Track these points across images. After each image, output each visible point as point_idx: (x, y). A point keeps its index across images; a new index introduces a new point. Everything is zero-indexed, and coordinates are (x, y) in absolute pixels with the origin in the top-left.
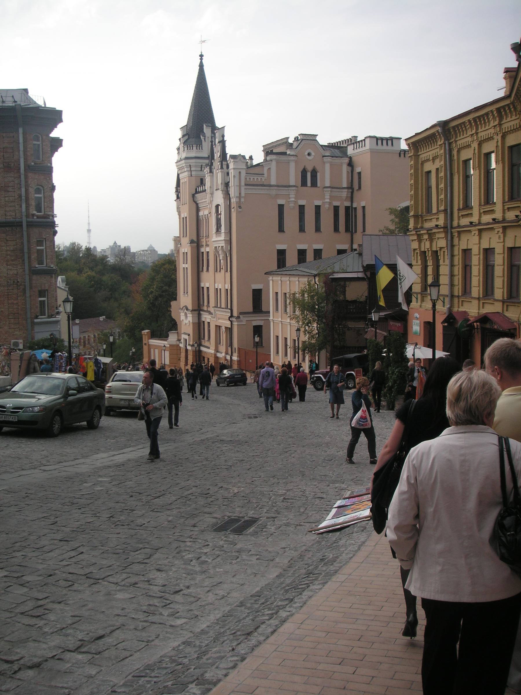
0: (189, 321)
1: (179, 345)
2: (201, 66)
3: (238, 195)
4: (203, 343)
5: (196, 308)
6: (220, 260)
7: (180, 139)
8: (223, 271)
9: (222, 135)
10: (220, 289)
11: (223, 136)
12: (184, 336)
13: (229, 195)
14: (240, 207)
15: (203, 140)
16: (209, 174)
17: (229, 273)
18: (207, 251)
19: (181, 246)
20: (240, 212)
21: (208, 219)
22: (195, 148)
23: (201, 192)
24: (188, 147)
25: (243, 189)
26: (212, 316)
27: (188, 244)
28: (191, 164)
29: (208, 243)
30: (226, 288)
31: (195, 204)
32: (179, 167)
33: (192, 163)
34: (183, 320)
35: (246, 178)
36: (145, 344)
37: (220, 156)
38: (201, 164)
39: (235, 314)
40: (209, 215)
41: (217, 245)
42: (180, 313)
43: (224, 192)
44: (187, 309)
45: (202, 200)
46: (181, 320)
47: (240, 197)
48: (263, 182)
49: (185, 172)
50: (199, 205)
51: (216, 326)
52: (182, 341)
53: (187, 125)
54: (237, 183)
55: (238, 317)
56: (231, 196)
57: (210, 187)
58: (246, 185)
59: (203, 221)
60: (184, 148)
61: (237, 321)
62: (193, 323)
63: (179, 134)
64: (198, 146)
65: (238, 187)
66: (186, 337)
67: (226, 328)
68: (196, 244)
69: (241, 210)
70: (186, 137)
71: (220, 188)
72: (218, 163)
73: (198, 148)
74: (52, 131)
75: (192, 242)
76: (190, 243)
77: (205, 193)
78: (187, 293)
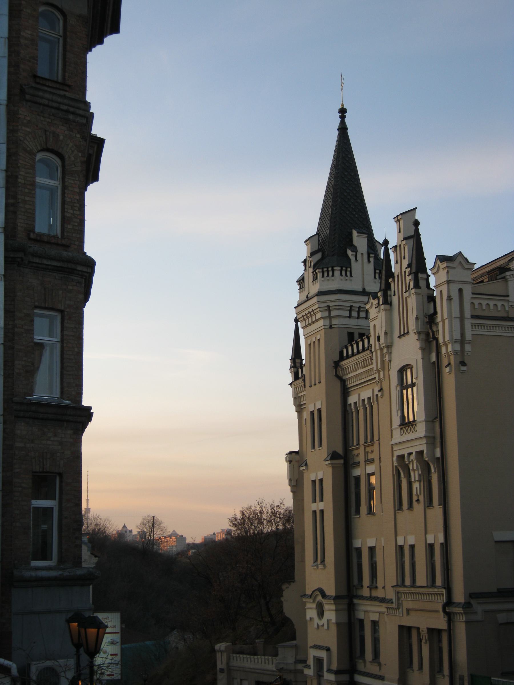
0: (328, 621)
1: (302, 672)
2: (343, 129)
3: (459, 337)
4: (361, 667)
5: (344, 592)
6: (410, 485)
7: (305, 262)
8: (419, 508)
9: (413, 220)
10: (412, 547)
11: (417, 223)
12: (313, 653)
13: (437, 340)
14: (463, 363)
15: (353, 259)
16: (382, 307)
17: (437, 511)
18: (367, 472)
19: (307, 469)
20: (463, 372)
21: (371, 407)
22: (337, 273)
23: (353, 355)
24: (323, 272)
25: (468, 323)
26: (390, 605)
27: (325, 461)
28: (331, 304)
29: (370, 456)
30: (430, 540)
31: (338, 383)
32: (304, 314)
33: (331, 301)
34: (311, 619)
35: (473, 303)
36: (222, 671)
37: (409, 266)
38: (349, 304)
39: (459, 596)
40: (380, 394)
41: (405, 452)
42: (304, 604)
43: (423, 336)
44: (324, 595)
45: (356, 371)
46: (308, 618)
47: (462, 341)
48: (508, 312)
49: (317, 321)
50: (348, 383)
51: (401, 628)
52: (311, 662)
53: (318, 234)
54: (456, 313)
55: (467, 606)
56: (441, 341)
57: (386, 333)
58: (473, 317)
59: (358, 412)
60: (315, 274)
61: (465, 613)
62: (338, 624)
63: (303, 252)
64: (344, 269)
65: (458, 320)
66: (323, 654)
67: (430, 631)
68: (342, 461)
69: (464, 368)
70: (319, 256)
71: (412, 326)
72: (408, 278)
73: (344, 273)
74: (91, 50)
75: (334, 456)
76: (331, 459)
77: (368, 352)
78: (323, 561)
